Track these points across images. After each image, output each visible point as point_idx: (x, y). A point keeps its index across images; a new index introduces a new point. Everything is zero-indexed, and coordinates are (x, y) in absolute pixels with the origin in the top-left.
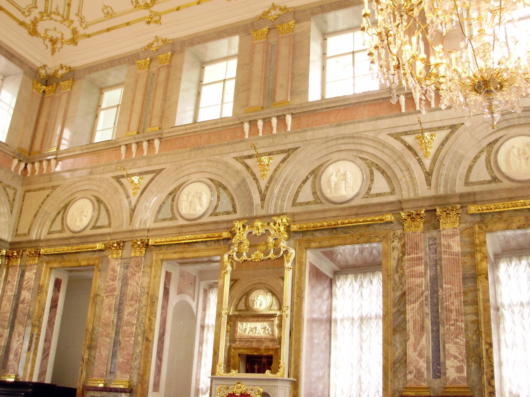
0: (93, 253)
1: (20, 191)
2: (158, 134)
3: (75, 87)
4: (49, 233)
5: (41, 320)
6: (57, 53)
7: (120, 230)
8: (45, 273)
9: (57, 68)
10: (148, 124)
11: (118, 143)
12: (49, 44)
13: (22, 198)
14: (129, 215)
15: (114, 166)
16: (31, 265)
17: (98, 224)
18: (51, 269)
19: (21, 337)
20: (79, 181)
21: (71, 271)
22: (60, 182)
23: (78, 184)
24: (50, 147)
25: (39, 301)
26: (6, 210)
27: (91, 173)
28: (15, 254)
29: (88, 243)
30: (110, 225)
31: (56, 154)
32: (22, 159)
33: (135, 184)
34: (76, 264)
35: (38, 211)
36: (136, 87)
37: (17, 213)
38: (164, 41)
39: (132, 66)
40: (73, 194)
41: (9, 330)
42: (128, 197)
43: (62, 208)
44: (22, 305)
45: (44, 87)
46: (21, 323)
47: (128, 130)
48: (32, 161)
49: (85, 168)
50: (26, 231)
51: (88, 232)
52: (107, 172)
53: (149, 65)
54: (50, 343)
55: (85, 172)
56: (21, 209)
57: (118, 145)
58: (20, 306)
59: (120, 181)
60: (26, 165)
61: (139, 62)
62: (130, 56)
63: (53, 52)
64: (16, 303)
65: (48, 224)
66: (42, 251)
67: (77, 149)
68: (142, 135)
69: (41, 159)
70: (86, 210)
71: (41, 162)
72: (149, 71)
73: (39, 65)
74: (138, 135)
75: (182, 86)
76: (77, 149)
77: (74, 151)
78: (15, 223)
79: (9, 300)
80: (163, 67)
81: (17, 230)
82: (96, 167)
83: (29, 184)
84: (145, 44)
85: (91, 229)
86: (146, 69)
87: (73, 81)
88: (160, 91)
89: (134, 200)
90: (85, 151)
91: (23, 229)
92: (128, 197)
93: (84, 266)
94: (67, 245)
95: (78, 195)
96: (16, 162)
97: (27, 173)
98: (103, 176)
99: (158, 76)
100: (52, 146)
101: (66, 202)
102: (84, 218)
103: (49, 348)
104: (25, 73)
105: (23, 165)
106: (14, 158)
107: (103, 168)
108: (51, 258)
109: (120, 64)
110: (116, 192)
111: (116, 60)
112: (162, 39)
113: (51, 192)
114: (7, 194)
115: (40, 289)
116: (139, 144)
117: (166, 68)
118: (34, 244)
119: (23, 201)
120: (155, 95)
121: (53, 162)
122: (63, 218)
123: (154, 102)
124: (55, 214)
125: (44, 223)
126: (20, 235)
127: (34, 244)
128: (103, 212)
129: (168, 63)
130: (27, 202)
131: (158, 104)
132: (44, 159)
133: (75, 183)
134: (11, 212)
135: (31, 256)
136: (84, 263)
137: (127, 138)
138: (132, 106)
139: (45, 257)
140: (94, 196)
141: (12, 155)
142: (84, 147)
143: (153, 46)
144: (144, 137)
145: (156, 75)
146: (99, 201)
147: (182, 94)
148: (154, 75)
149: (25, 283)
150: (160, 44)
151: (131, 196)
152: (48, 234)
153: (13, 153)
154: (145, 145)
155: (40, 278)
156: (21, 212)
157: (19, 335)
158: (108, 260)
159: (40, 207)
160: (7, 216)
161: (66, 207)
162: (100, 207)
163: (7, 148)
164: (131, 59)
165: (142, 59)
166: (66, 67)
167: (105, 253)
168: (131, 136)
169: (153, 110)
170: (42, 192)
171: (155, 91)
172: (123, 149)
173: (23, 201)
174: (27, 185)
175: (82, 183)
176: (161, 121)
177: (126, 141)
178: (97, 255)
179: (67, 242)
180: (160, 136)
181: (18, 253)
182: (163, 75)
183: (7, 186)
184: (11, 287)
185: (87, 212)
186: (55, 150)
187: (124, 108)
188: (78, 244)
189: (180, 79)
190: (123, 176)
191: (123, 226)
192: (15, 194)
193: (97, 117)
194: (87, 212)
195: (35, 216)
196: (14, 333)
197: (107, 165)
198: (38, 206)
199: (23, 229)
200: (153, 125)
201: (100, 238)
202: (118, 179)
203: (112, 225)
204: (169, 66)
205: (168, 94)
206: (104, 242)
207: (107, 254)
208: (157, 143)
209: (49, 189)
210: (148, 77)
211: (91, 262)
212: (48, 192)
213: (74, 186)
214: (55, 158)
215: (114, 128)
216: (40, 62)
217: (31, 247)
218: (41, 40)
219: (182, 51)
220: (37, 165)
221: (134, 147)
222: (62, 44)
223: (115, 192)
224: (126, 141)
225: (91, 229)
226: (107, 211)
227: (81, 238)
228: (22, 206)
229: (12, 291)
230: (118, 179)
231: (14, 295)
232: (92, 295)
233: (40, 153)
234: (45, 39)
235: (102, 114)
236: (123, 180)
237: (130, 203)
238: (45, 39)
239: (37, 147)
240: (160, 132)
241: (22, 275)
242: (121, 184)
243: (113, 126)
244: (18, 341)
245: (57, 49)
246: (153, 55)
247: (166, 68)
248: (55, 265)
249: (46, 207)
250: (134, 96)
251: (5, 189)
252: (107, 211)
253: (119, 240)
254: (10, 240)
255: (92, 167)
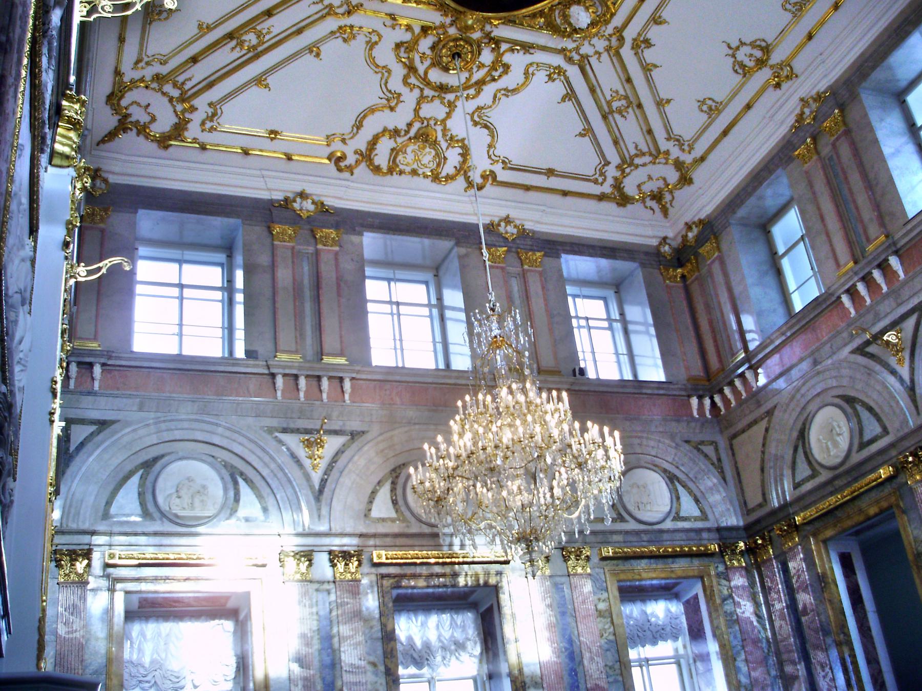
0: (881, 488)
1: (723, 444)
2: (889, 247)
3: (724, 246)
4: (796, 486)
5: (846, 631)
6: (671, 211)
7: (906, 430)
8: (819, 552)
9: (684, 233)
10: (864, 240)
11: (832, 294)
12: (654, 204)
13: (730, 453)
14: (908, 400)
15: (845, 335)
16: (791, 549)
17: (867, 437)
18: (825, 542)
19: (827, 669)
20: (804, 384)
21: (857, 533)
22: (774, 401)
23: (803, 391)
24: (734, 354)
25: (830, 601)
26: (715, 481)
27: (816, 363)
28: (760, 542)
29: (864, 475)
30: (885, 431)
31: (747, 359)
32: (701, 393)
33: (895, 345)
34: (861, 518)
35: (763, 461)
36: (814, 193)
37: (733, 477)
38: (818, 97)
39: (791, 166)
40: (804, 408)
41: (803, 663)
42: (893, 372)
43: (798, 439)
44: (806, 617)
45: (679, 270)
46: (817, 647)
47: (838, 265)
48: (718, 388)
49: (802, 360)
50: (759, 499)
51: (856, 458)
52: (839, 349)
53: (815, 148)
54: (878, 663)
55: (805, 366)
56: (737, 468)
57: (834, 299)
58: (803, 619)
59: (868, 353)
60: (712, 398)
61: (796, 153)
62: (779, 151)
63: (665, 212)
64: (794, 617)
65: (787, 472)
66: (798, 519)
67: (774, 336)
68: (865, 261)
69: (728, 380)
70: (835, 424)
71: (731, 384)
72: (820, 158)
73: (655, 242)
74: (859, 266)
75: (887, 150)
76: (774, 336)
77: (772, 342)
78: (738, 495)
79: (782, 617)
80: (837, 139)
81: (745, 503)
82: (818, 349)
83: (730, 425)
84: (791, 120)
85: (858, 452)
86: (815, 157)
87: (716, 238)
88: (855, 179)
89: (904, 372)
90: (789, 334)
91: (754, 499)
92: (893, 372)
93: (876, 515)
94: (832, 494)
95: (812, 407)
96: (694, 401)
97: (720, 411)
98: (835, 357)
99: (838, 157)
100: (735, 351)
101: (799, 426)
102: (838, 438)
103: (880, 671)
104: (643, 265)
105: (707, 402)
106: (689, 396)
107: (829, 345)
108: (817, 525)
109: (771, 172)
110: (870, 372)
111: (761, 170)
112: (812, 97)
113: (769, 422)
114: (706, 456)
115: (822, 583)
116: (867, 279)
117: (843, 138)
118: (781, 515)
119: (733, 455)
120: (850, 190)
121: (749, 375)
122: (805, 453)
123: (854, 201)
124: (791, 452)
125: (782, 475)
126: (753, 510)
127: (781, 515)
128: (865, 415)
129: (842, 129)
130: (740, 456)
131: (862, 199)
132: (732, 376)
133: (798, 390)
134: (724, 479)
135: (787, 535)
136: (872, 511)
137: (842, 280)
138: (825, 225)
139: (808, 528)
140: (838, 397)
141: (683, 393)
142: (784, 328)
143: (805, 116)
144: (870, 262)
145: (835, 157)
146: (850, 400)
147: (892, 164)
148: (830, 159)
149: (794, 581)
150: (814, 106)
151: (898, 368)
152: (795, 488)
153: (685, 390)
154: (877, 275)
155: (815, 564)
156: (738, 474)
157: (823, 668)
158: (911, 489)
159: (763, 452)
160: (721, 490)
161: (803, 435)
162: (855, 410)
163: (672, 386)
164: (781, 157)
165: (799, 147)
166: (694, 223)
167: (901, 479)
168: (847, 272)
169: (859, 214)
170: (755, 428)
171: (848, 183)
172: (845, 299)
173: (733, 455)
174: (727, 428)
175: (809, 384)
176: (882, 224)
177: (843, 285)
178: (888, 489)
179: (830, 489)
180: (894, 249)
181: (763, 538)
182: (845, 151)
183: (700, 444)
184: (776, 596)
185: (839, 427)
186: (743, 355)
187: (812, 234)
188: (849, 484)
189: (876, 141)
190: (868, 343)
191: (908, 422)
192: (717, 450)
193: (779, 273)
194: (839, 427)
195: (762, 470)
196: (813, 667)
197: (834, 336)
198: (760, 453)
199: (754, 499)
200: (872, 236)
201: (880, 459)
202: (861, 350)
203: (890, 429)
204: (848, 132)
205: (871, 176)
206: (890, 463)
207: (904, 480)
208: (894, 262)
209: (762, 419)
210: (824, 168)
211: (884, 504)
212: (763, 424)
213: (798, 396)
214: (748, 369)
215: (815, 275)
216: (654, 237)
217: (778, 521)
218: (638, 206)
219: (854, 96)
220: (727, 391)
221: (861, 287)
222: (671, 192)
223: (869, 374)
224: (843, 285)
225: (858, 452)
226: (870, 409)
227: (848, 472)
228: (736, 463)
229: (780, 601)
230: (861, 350)
231: (787, 607)
232: (910, 557)
233: (723, 370)
234: (643, 200)
235: (785, 263)
236: (871, 349)
237: (901, 380)
238: (643, 200)
239: (714, 363)
240: (890, 241)
241: (785, 570)
242: (872, 356)
243: (811, 273)
244: (824, 677)
245: (668, 205)
246: (812, 130)
247: (843, 138)
248: (829, 533)
249: (772, 449)
250: (819, 209)
251: (699, 450)
252: (870, 409)
253: (912, 449)
254: (741, 523)
255: (813, 353)
